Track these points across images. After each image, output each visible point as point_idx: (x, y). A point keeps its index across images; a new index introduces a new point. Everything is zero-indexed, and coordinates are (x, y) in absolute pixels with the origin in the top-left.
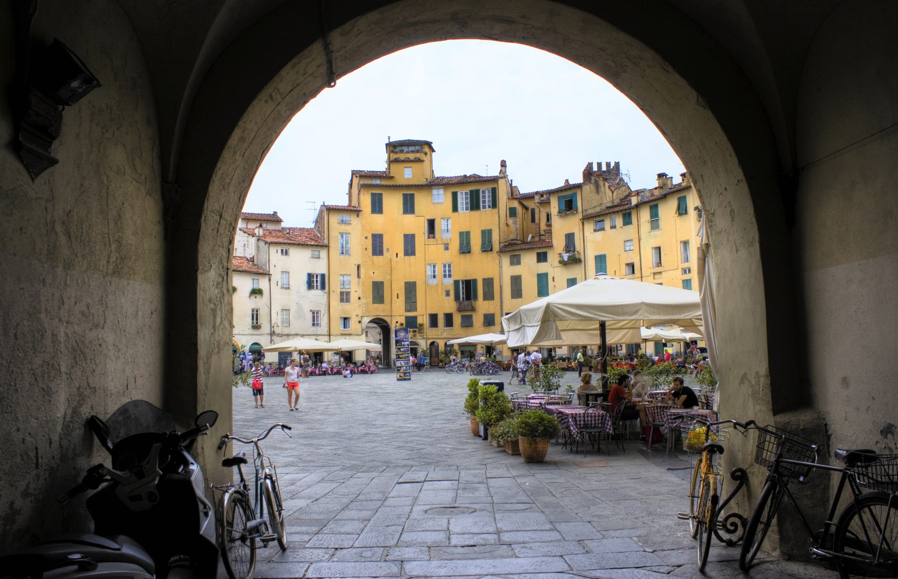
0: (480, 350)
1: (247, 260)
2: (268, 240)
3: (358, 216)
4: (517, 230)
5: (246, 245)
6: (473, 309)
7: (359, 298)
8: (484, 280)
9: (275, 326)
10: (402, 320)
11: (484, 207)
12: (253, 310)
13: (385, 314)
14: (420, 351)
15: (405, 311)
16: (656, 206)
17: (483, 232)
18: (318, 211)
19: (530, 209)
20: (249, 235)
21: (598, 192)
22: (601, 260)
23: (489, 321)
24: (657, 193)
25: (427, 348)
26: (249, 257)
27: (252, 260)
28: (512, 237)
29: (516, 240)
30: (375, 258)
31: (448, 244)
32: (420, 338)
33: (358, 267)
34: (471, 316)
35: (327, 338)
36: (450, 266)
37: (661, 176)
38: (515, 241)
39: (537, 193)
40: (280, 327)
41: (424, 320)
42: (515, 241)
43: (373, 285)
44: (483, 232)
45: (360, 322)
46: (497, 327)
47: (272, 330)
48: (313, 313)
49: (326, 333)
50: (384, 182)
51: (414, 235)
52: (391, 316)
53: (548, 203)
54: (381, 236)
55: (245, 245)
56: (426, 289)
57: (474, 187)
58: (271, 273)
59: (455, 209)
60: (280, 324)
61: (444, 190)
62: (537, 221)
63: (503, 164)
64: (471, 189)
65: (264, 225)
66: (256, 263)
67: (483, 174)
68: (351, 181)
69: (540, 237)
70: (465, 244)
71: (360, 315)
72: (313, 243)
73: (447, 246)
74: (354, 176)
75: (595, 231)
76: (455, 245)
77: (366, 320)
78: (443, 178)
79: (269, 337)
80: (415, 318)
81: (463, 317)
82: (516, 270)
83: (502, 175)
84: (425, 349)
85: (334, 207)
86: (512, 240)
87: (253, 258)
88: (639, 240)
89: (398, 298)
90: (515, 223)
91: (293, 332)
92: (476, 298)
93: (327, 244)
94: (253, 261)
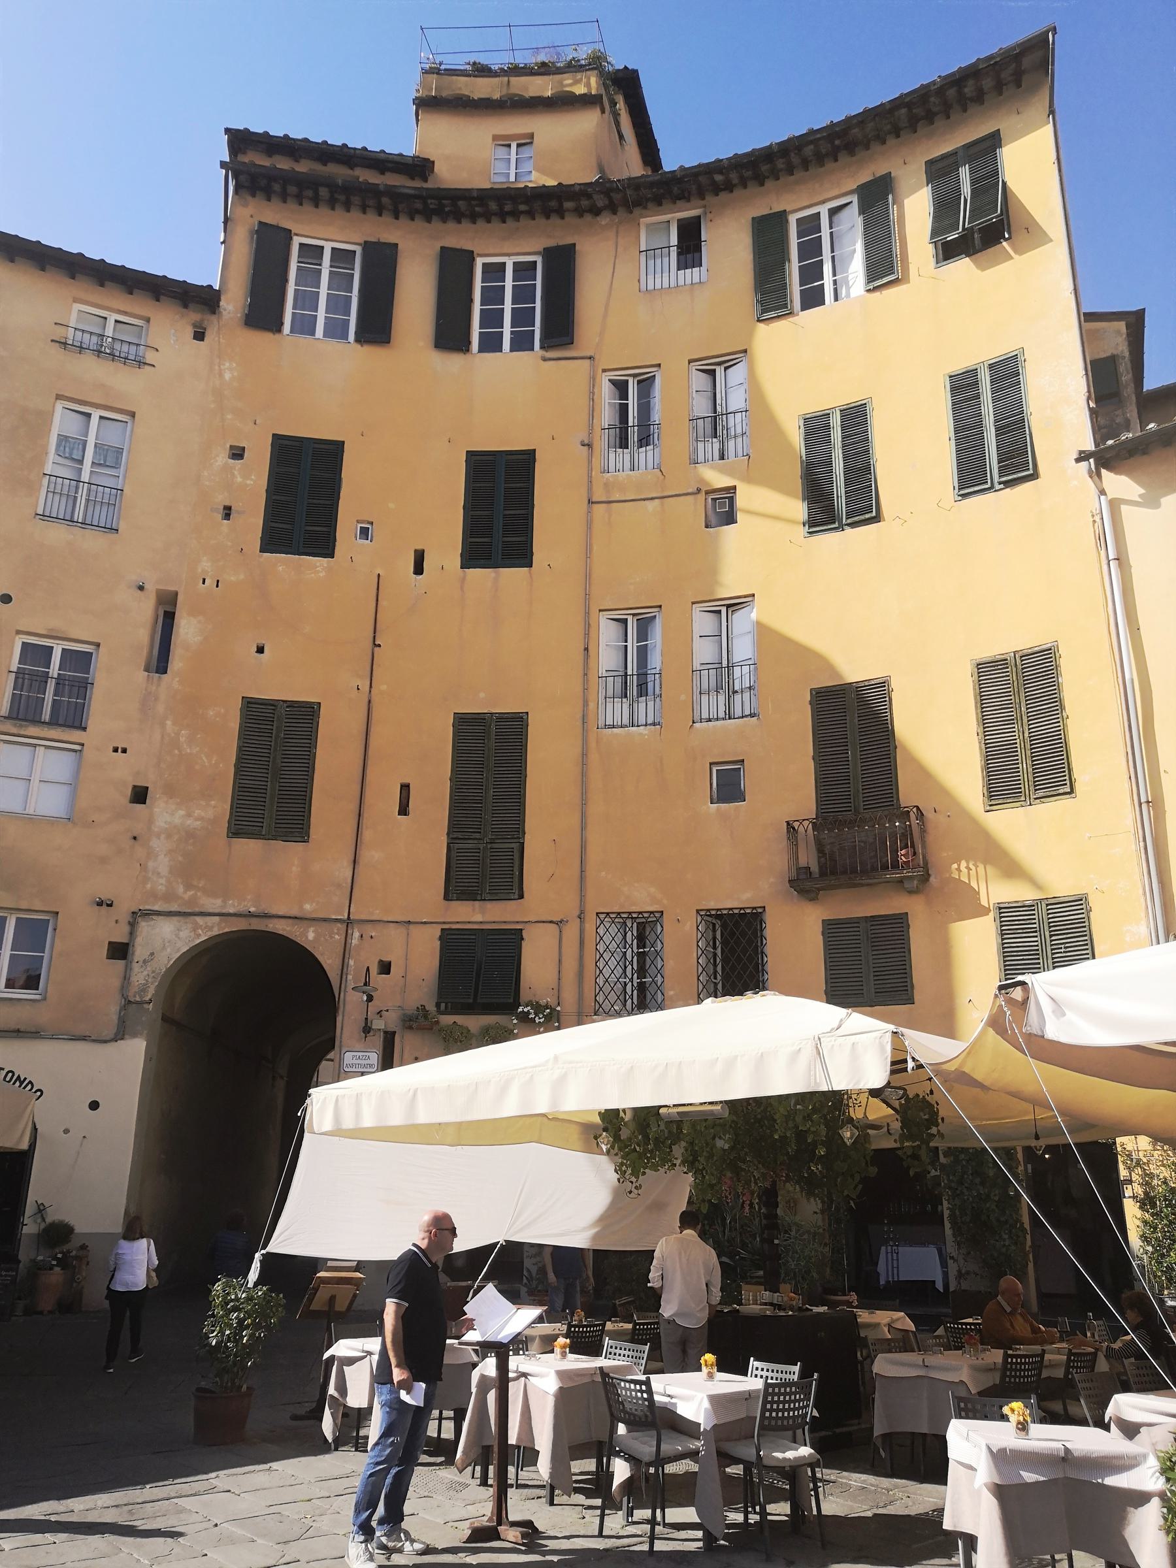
3: (199, 336)
7: (140, 795)
15: (447, 897)
30: (283, 564)
34: (898, 925)
45: (120, 951)
52: (349, 922)
56: (584, 755)
81: (832, 929)
89: (404, 810)
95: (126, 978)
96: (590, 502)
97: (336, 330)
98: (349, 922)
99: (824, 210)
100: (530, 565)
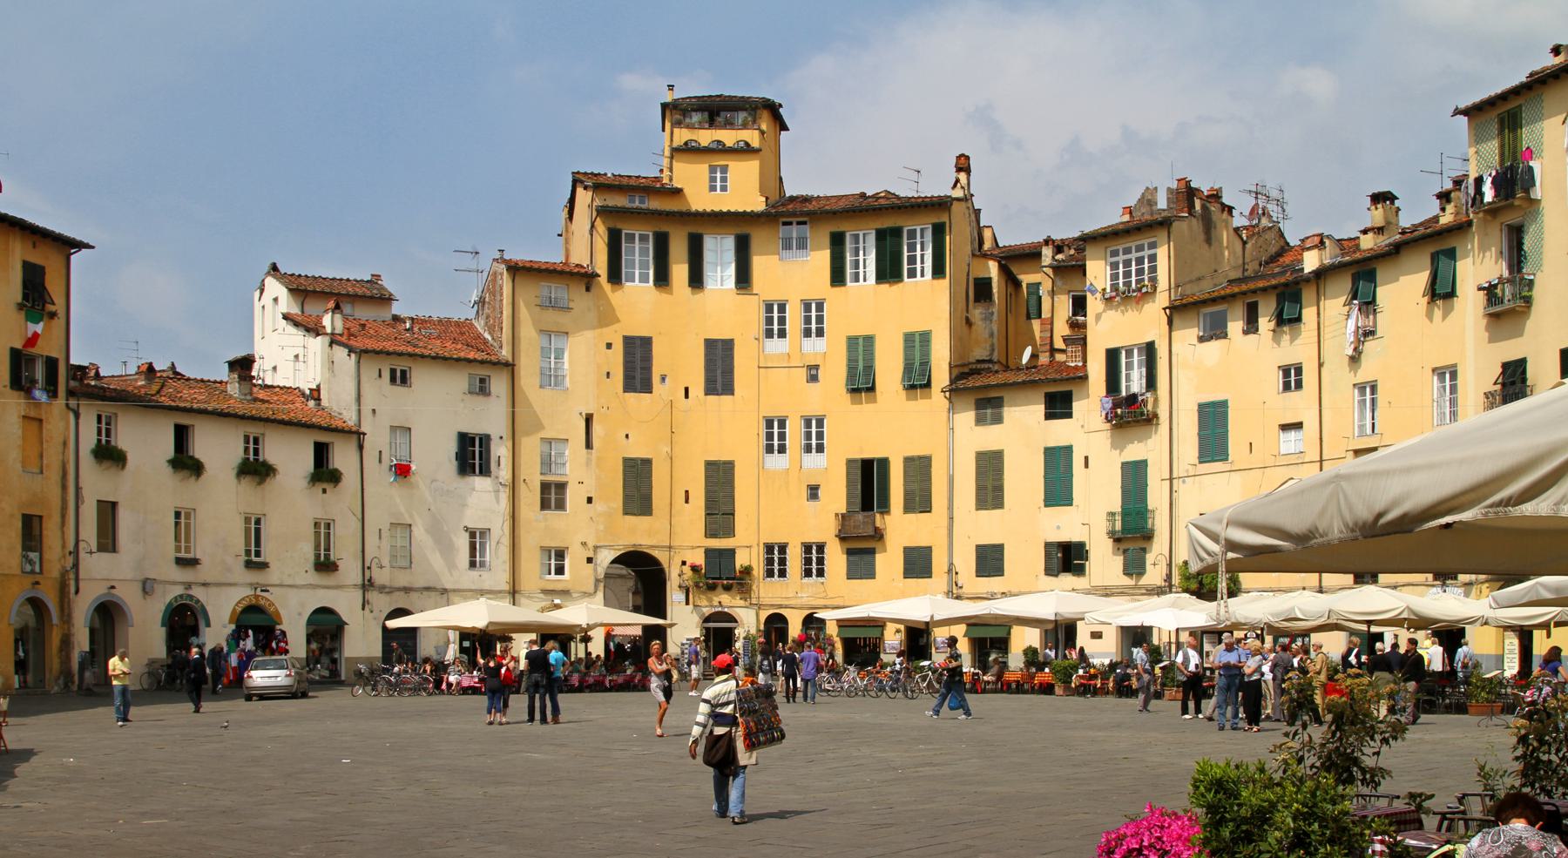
0: (893, 639)
1: (303, 394)
2: (358, 343)
3: (588, 289)
4: (992, 335)
5: (301, 358)
6: (878, 535)
7: (590, 500)
8: (908, 461)
9: (374, 567)
10: (699, 559)
11: (912, 274)
12: (317, 525)
13: (653, 542)
14: (740, 632)
15: (706, 536)
16: (1371, 277)
17: (909, 338)
18: (485, 274)
19: (1024, 286)
20: (308, 330)
21: (1208, 240)
22: (1213, 419)
23: (918, 563)
24: (1368, 242)
25: (759, 631)
26: (306, 385)
27: (315, 394)
28: (980, 353)
29: (990, 361)
30: (631, 396)
31: (817, 367)
32: (742, 603)
33: (589, 420)
35: (508, 598)
36: (820, 423)
37: (1379, 198)
38: (986, 366)
39: (1047, 242)
40: (387, 570)
41: (748, 556)
42: (983, 366)
43: (625, 466)
44: (909, 338)
46: (939, 579)
47: (367, 577)
48: (473, 535)
49: (505, 587)
50: (654, 204)
51: (732, 340)
52: (670, 547)
53: (1071, 270)
54: (646, 342)
55: (297, 357)
57: (888, 222)
58: (363, 429)
59: (838, 277)
60: (386, 562)
61: (811, 228)
62: (1046, 314)
63: (963, 165)
64: (879, 226)
65: (347, 309)
66: (325, 402)
67: (905, 190)
68: (572, 201)
69: (1052, 355)
70: (861, 367)
71: (591, 544)
72: (471, 356)
73: (814, 372)
74: (580, 191)
75: (1201, 339)
76: (836, 372)
77: (606, 557)
78: (806, 199)
79: (360, 593)
80: (731, 553)
82: (990, 437)
83: (958, 193)
84: (753, 631)
85: (528, 265)
86: (979, 362)
87: (318, 389)
88: (1320, 365)
89: (687, 501)
90: (988, 318)
91: (421, 583)
92: (885, 507)
93: (510, 360)
94: (318, 399)
95: (595, 570)
96: (759, 367)
97: (644, 279)
98: (670, 547)
99: (861, 234)
100: (733, 394)
